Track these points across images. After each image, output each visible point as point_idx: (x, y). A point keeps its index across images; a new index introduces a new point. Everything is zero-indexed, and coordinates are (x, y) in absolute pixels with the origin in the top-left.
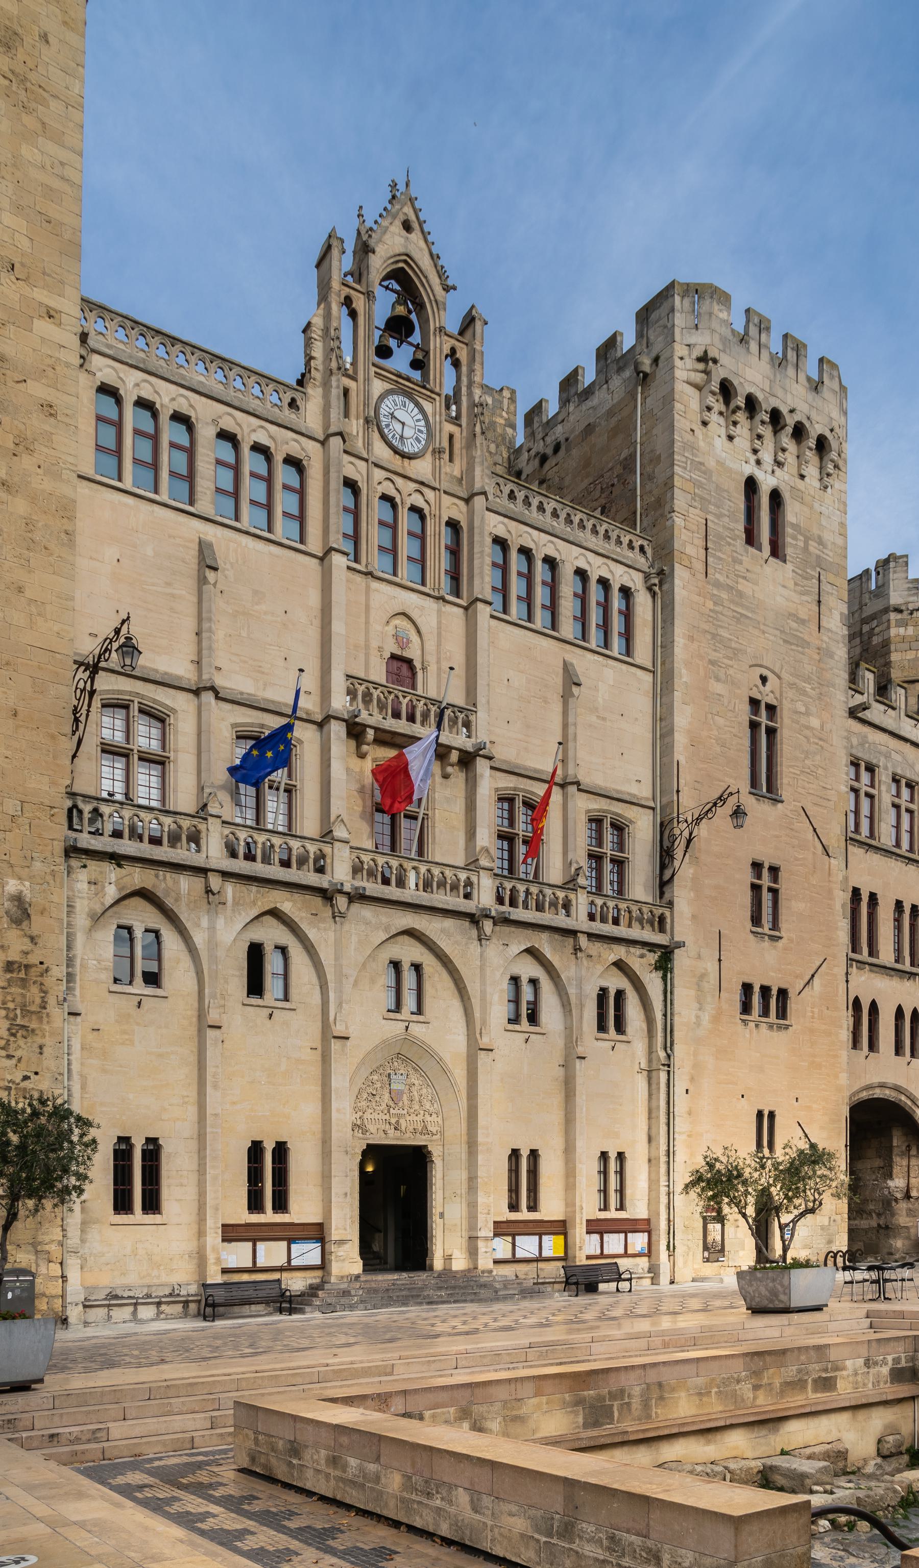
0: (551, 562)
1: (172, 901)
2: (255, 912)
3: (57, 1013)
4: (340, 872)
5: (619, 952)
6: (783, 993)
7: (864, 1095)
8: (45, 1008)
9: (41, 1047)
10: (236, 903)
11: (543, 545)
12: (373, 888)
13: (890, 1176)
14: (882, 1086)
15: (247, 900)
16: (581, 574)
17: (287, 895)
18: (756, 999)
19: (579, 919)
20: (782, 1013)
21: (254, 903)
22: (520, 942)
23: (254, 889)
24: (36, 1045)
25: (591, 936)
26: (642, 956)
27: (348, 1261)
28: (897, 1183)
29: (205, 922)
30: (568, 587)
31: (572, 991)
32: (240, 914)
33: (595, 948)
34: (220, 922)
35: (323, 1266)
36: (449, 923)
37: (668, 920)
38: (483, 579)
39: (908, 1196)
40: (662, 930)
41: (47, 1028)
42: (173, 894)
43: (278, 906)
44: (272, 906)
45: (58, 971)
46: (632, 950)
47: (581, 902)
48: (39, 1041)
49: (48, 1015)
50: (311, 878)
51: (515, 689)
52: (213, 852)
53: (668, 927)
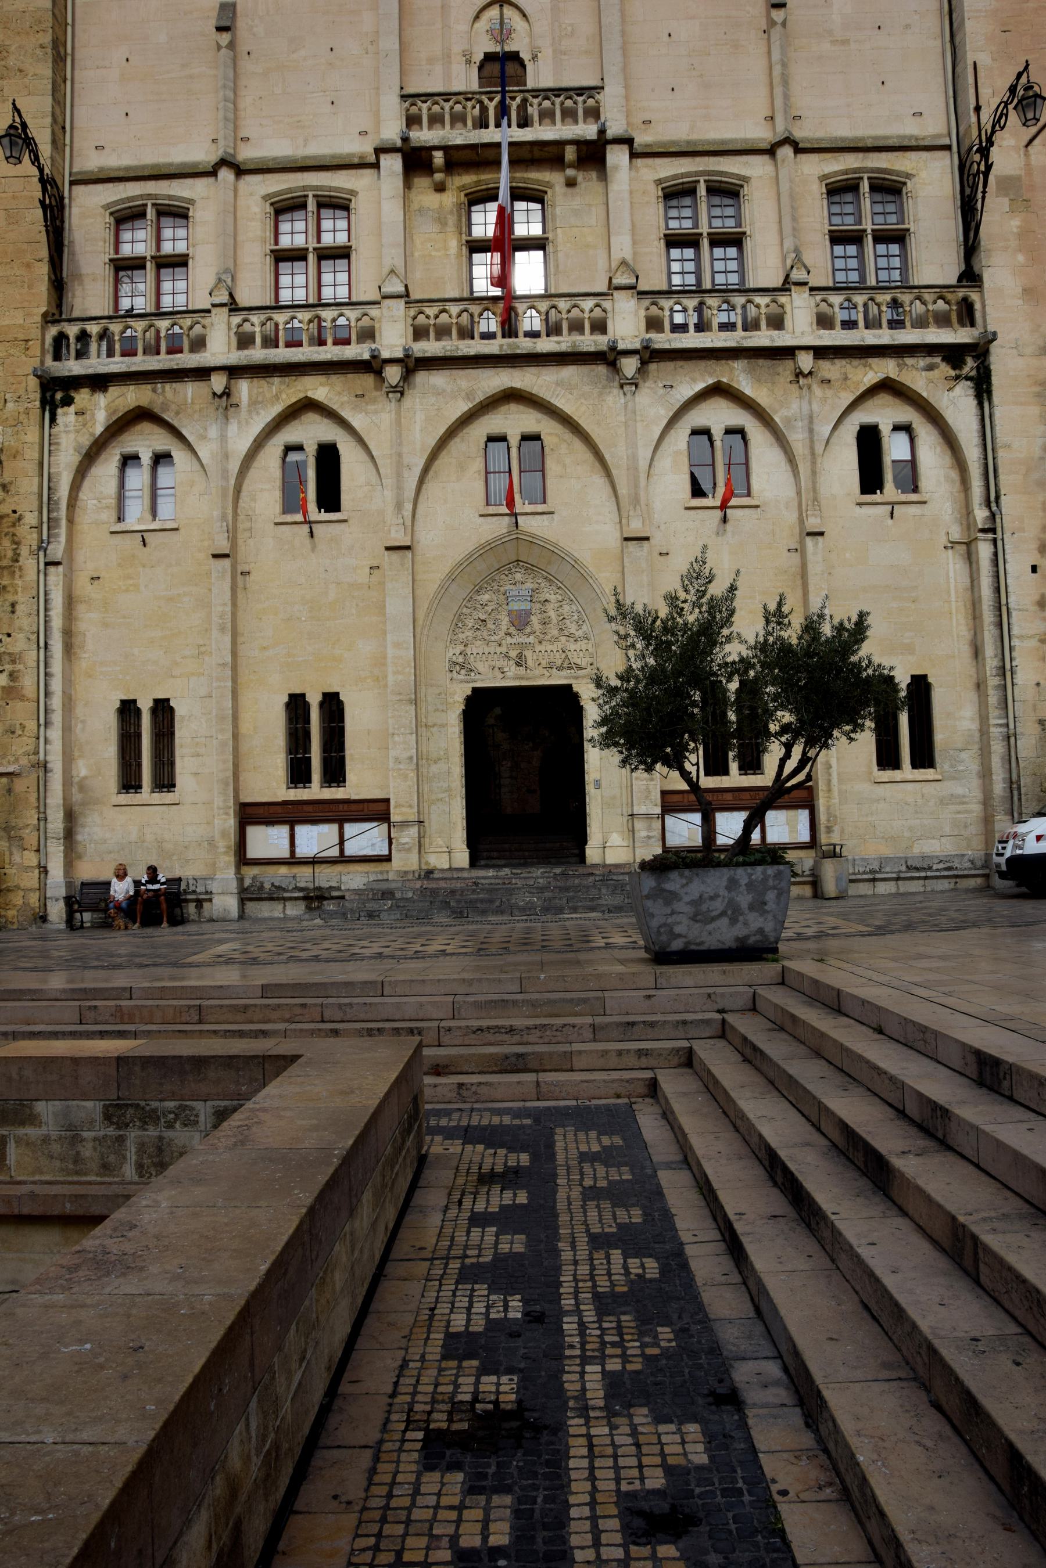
1: (172, 414)
2: (276, 409)
3: (29, 565)
5: (886, 368)
8: (17, 561)
9: (13, 605)
10: (254, 403)
15: (268, 395)
17: (322, 379)
21: (277, 397)
22: (694, 380)
23: (276, 380)
24: (8, 603)
25: (821, 352)
26: (930, 368)
29: (213, 432)
32: (258, 413)
33: (830, 369)
34: (233, 428)
37: (978, 306)
40: (973, 324)
41: (19, 582)
42: (173, 407)
43: (310, 394)
44: (301, 395)
45: (31, 519)
46: (909, 361)
48: (11, 598)
49: (20, 569)
53: (978, 315)
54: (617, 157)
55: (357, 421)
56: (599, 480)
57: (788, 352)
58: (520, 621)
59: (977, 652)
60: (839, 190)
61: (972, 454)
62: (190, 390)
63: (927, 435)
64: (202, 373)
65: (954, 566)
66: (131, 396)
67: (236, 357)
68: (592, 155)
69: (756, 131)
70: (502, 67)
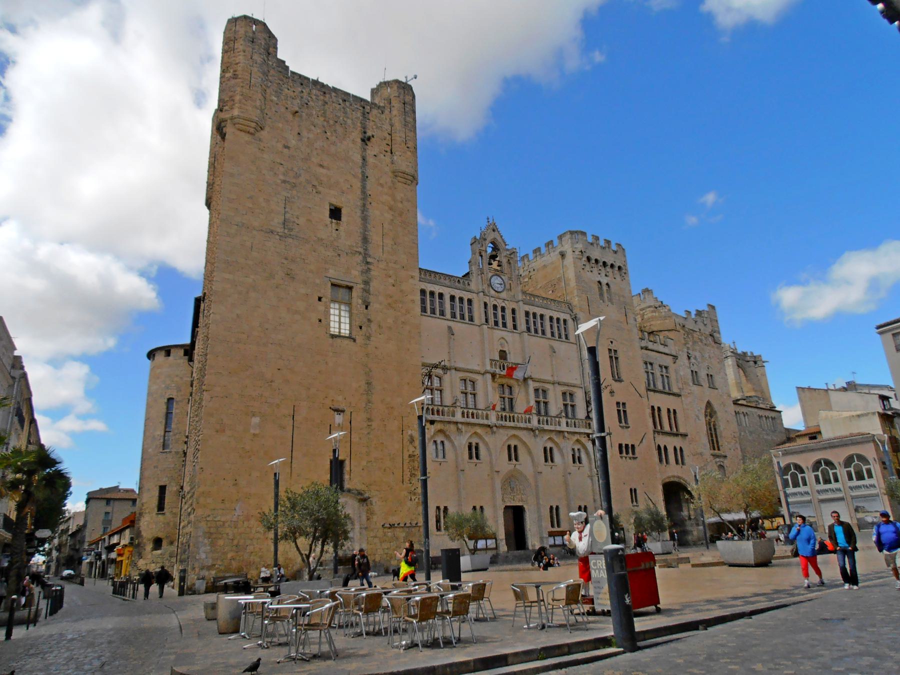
0: (542, 316)
4: (493, 420)
6: (633, 446)
7: (667, 480)
11: (539, 311)
12: (503, 423)
13: (681, 510)
14: (674, 477)
16: (551, 318)
18: (624, 449)
19: (563, 427)
20: (633, 453)
27: (503, 548)
28: (685, 513)
30: (547, 323)
31: (564, 451)
35: (496, 548)
36: (525, 432)
38: (522, 326)
39: (690, 519)
40: (590, 428)
47: (563, 421)
50: (485, 422)
51: (537, 356)
52: (458, 417)
54: (530, 382)
55: (486, 439)
56: (529, 458)
57: (563, 432)
58: (512, 489)
59: (595, 501)
60: (564, 394)
61: (593, 457)
62: (453, 427)
63: (582, 451)
64: (457, 423)
65: (589, 481)
66: (438, 426)
67: (463, 420)
68: (525, 380)
69: (549, 378)
70: (503, 355)
